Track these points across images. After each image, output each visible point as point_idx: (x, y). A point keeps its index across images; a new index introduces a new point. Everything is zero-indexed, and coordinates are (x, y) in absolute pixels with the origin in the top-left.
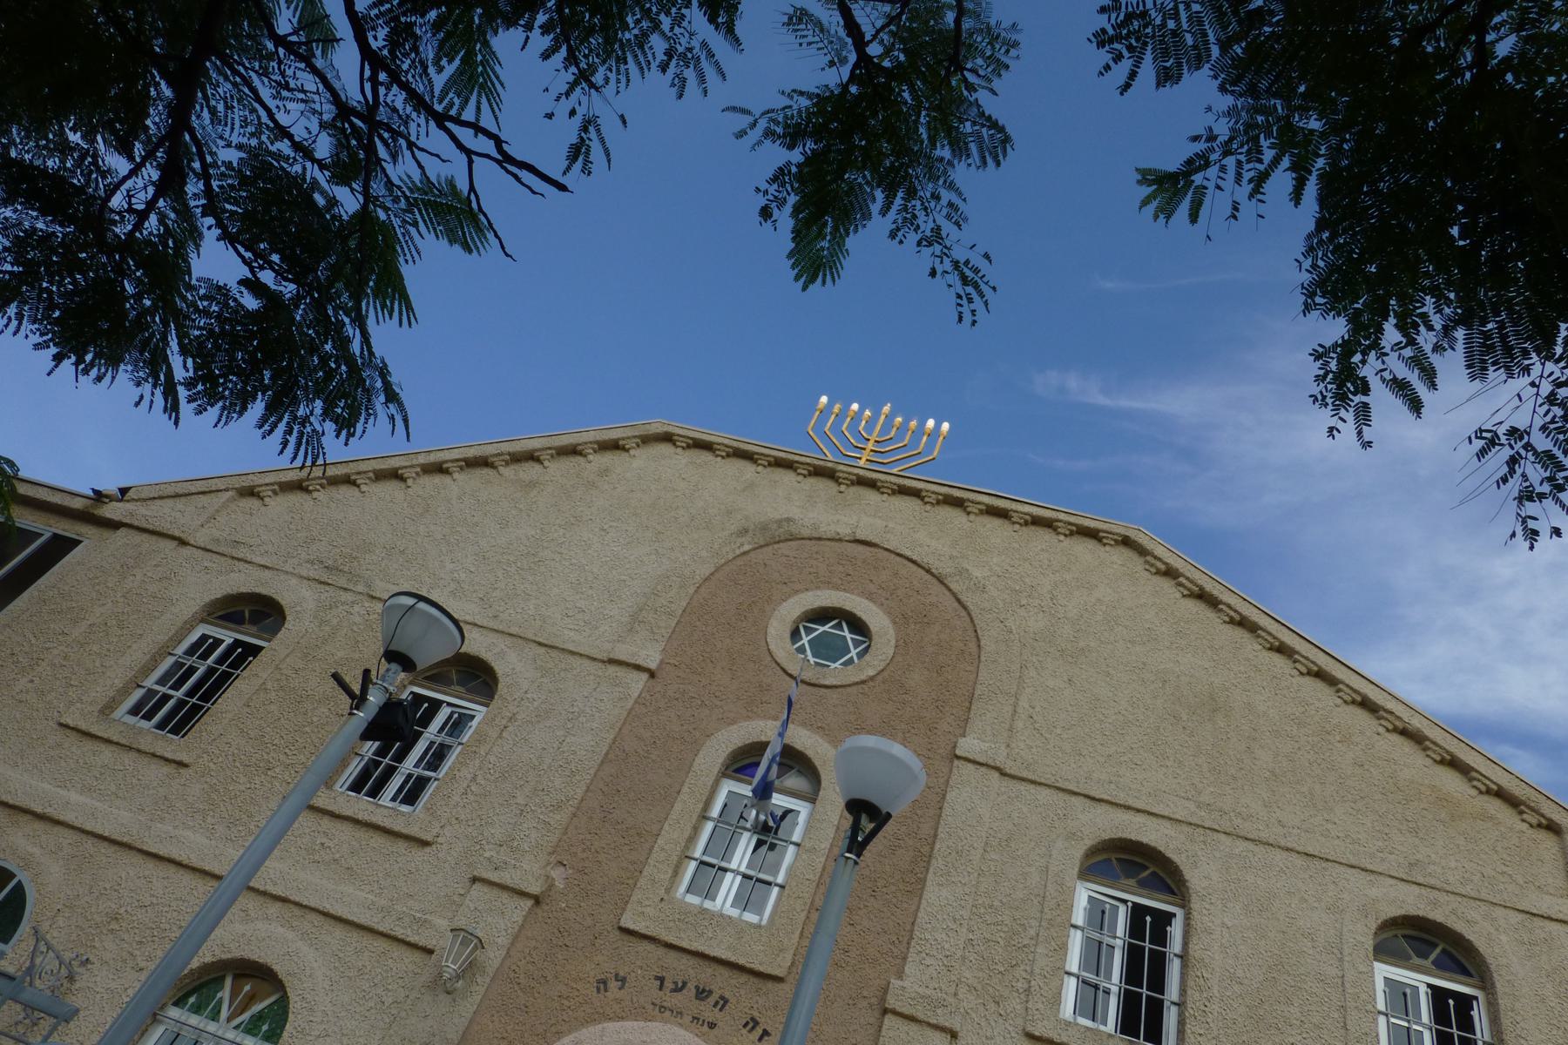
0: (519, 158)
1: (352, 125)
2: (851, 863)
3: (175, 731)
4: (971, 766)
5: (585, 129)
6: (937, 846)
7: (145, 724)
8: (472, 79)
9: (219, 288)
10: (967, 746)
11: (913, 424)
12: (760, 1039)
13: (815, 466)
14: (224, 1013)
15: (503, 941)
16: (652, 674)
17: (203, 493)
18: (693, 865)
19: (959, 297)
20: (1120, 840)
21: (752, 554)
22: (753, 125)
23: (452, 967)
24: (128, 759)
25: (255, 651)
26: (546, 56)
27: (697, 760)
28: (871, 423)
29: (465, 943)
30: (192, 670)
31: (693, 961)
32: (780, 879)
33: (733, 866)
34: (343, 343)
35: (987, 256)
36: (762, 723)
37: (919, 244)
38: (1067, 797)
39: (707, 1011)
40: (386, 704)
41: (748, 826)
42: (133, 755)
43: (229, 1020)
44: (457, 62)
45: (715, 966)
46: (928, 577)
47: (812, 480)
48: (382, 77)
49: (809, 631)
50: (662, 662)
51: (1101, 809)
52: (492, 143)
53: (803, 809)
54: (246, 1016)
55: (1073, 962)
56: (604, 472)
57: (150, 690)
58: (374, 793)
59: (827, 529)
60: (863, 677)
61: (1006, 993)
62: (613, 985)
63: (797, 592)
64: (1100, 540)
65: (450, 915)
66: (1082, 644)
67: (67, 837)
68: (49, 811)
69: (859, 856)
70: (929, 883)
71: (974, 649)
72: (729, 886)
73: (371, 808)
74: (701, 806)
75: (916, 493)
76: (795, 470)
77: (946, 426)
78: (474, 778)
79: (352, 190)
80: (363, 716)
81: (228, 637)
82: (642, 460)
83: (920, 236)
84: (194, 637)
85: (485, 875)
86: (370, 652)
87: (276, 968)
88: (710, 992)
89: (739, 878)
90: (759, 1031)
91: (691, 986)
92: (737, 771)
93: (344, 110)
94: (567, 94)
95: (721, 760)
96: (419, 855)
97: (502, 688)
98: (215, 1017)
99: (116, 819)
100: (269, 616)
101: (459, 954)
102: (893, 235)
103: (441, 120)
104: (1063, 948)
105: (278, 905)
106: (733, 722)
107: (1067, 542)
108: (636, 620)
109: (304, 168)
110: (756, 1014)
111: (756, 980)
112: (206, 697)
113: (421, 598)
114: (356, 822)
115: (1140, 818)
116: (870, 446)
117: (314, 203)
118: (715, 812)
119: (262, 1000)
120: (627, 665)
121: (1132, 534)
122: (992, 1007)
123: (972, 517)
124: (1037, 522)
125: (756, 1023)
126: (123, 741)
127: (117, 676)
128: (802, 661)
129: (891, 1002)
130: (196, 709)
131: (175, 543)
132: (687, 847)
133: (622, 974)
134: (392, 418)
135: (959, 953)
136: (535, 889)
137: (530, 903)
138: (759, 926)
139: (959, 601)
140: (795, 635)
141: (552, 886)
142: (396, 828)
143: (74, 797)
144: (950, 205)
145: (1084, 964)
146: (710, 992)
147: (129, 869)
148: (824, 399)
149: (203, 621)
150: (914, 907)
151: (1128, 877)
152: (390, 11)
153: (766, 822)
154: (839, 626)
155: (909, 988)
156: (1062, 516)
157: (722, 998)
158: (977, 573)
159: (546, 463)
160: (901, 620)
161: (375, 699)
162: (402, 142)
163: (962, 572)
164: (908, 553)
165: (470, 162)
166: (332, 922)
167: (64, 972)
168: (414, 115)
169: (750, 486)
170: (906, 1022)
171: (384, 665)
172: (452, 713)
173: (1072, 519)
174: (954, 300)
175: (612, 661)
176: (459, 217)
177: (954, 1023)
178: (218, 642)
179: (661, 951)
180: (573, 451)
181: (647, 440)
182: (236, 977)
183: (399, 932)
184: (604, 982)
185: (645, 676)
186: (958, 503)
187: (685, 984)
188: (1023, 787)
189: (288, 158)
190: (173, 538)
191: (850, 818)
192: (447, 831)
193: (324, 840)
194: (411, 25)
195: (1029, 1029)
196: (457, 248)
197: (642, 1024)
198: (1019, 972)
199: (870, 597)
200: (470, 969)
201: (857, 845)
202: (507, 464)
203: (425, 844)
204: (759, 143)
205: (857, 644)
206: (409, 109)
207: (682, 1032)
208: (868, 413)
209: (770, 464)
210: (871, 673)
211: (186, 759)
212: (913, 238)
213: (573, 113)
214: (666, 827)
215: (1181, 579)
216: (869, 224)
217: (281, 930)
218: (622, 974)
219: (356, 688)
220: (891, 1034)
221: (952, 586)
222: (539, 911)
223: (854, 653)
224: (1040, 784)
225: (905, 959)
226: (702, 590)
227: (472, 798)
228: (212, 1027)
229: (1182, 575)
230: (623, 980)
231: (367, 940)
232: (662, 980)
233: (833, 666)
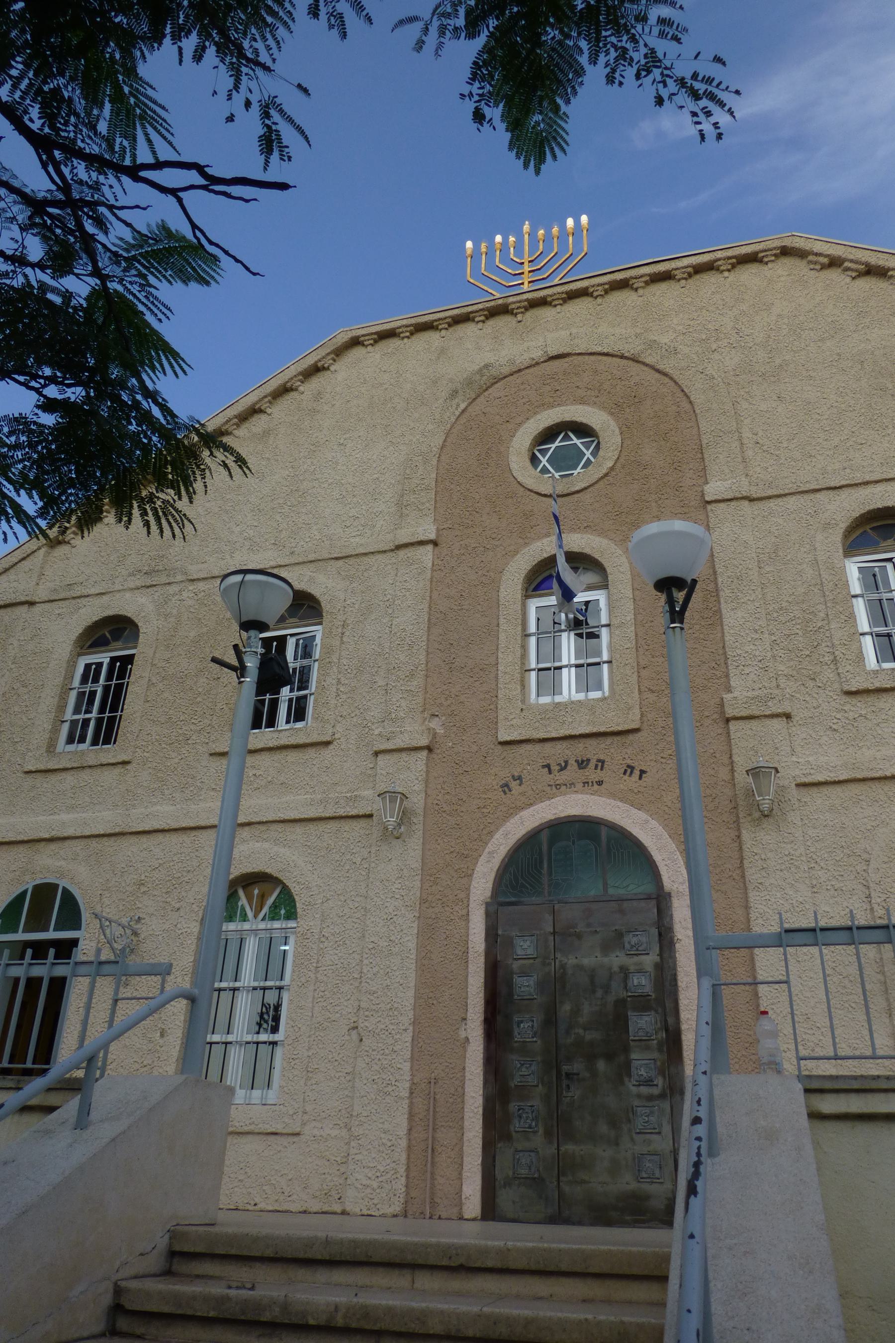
0: (228, 176)
1: (50, 216)
2: (678, 630)
3: (107, 741)
4: (722, 505)
5: (266, 115)
6: (720, 580)
7: (82, 747)
8: (129, 112)
9: (16, 419)
10: (713, 489)
11: (555, 230)
12: (640, 778)
13: (487, 309)
14: (250, 914)
15: (419, 787)
16: (435, 543)
17: (24, 559)
18: (533, 674)
19: (694, 114)
20: (869, 512)
21: (470, 409)
22: (426, 30)
23: (392, 821)
24: (85, 775)
25: (130, 659)
26: (198, 57)
27: (502, 595)
28: (518, 246)
29: (393, 800)
30: (93, 694)
31: (565, 744)
32: (605, 657)
33: (565, 662)
34: (146, 418)
35: (718, 60)
36: (539, 544)
37: (638, 76)
38: (812, 496)
39: (592, 774)
40: (261, 664)
41: (563, 627)
42: (88, 771)
43: (255, 917)
44: (108, 106)
45: (583, 740)
46: (624, 362)
47: (491, 322)
48: (57, 153)
49: (543, 452)
50: (438, 530)
51: (844, 493)
52: (194, 173)
53: (600, 596)
54: (266, 909)
55: (864, 624)
56: (318, 396)
57: (71, 721)
58: (271, 723)
59: (524, 359)
60: (604, 471)
61: (818, 669)
62: (514, 784)
63: (520, 425)
64: (761, 261)
65: (371, 785)
66: (778, 361)
67: (77, 846)
68: (54, 833)
69: (682, 622)
70: (724, 611)
71: (687, 406)
72: (568, 678)
73: (275, 735)
74: (520, 628)
75: (583, 293)
76: (473, 320)
77: (584, 219)
78: (339, 682)
79: (77, 275)
80: (250, 680)
81: (104, 658)
82: (343, 371)
83: (635, 67)
84: (80, 669)
85: (383, 747)
86: (234, 634)
87: (268, 871)
88: (588, 760)
89: (573, 670)
90: (637, 773)
91: (572, 761)
92: (535, 589)
93: (37, 205)
94: (236, 87)
95: (520, 587)
96: (327, 753)
97: (325, 606)
98: (244, 918)
99: (103, 819)
100: (125, 629)
101: (392, 810)
102: (610, 79)
103: (134, 172)
104: (852, 617)
105: (247, 828)
106: (516, 552)
107: (732, 277)
108: (401, 507)
109: (26, 276)
110: (629, 762)
111: (619, 738)
112: (114, 709)
113: (245, 572)
115: (880, 488)
116: (527, 268)
117: (50, 303)
118: (532, 628)
119: (271, 895)
120: (412, 544)
121: (787, 242)
122: (811, 684)
123: (640, 291)
124: (699, 269)
125: (632, 768)
126: (75, 765)
127: (44, 723)
128: (548, 480)
129: (730, 712)
130: (112, 720)
131: (26, 607)
132: (523, 664)
133: (516, 774)
134: (225, 465)
135: (769, 654)
136: (424, 742)
137: (425, 753)
138: (604, 699)
139: (658, 371)
140: (534, 460)
141: (435, 735)
142: (301, 742)
143: (65, 817)
144: (662, 21)
145: (873, 622)
146: (588, 760)
147: (131, 848)
148: (469, 244)
149: (79, 655)
150: (719, 635)
151: (885, 539)
152: (30, 85)
153: (575, 618)
154: (567, 438)
155: (741, 693)
156: (719, 255)
157: (599, 761)
158: (664, 339)
159: (269, 411)
160: (615, 410)
161: (252, 663)
162: (102, 209)
163: (652, 345)
164: (599, 349)
165: (180, 201)
166: (291, 824)
167: (128, 932)
168: (102, 178)
169: (443, 351)
170: (747, 722)
171: (244, 634)
172: (298, 640)
173: (730, 253)
174: (689, 118)
175: (399, 547)
176: (184, 256)
177: (786, 707)
178: (100, 665)
179: (538, 747)
180: (284, 390)
181: (339, 352)
182: (244, 888)
183: (341, 812)
184: (507, 785)
185: (430, 547)
186: (623, 285)
187: (566, 762)
188: (772, 503)
189: (7, 273)
191: (663, 597)
192: (339, 728)
193: (254, 772)
194: (56, 91)
195: (846, 688)
196: (193, 285)
197: (548, 802)
198: (823, 649)
199: (582, 401)
200: (405, 817)
201: (677, 615)
202: (238, 425)
203: (327, 743)
204: (440, 46)
205: (587, 445)
206: (94, 175)
207: (580, 796)
208: (512, 239)
209: (450, 325)
210: (610, 464)
211: (126, 758)
212: (630, 72)
213: (248, 104)
214: (500, 655)
215: (846, 264)
216: (585, 79)
217: (258, 845)
218: (516, 774)
219: (234, 662)
220: (739, 734)
221: (647, 361)
222: (434, 756)
223: (588, 454)
224: (785, 495)
225: (727, 676)
226: (443, 458)
227: (345, 696)
228: (246, 926)
229: (845, 260)
230: (520, 778)
231: (322, 826)
232: (548, 766)
233: (575, 472)
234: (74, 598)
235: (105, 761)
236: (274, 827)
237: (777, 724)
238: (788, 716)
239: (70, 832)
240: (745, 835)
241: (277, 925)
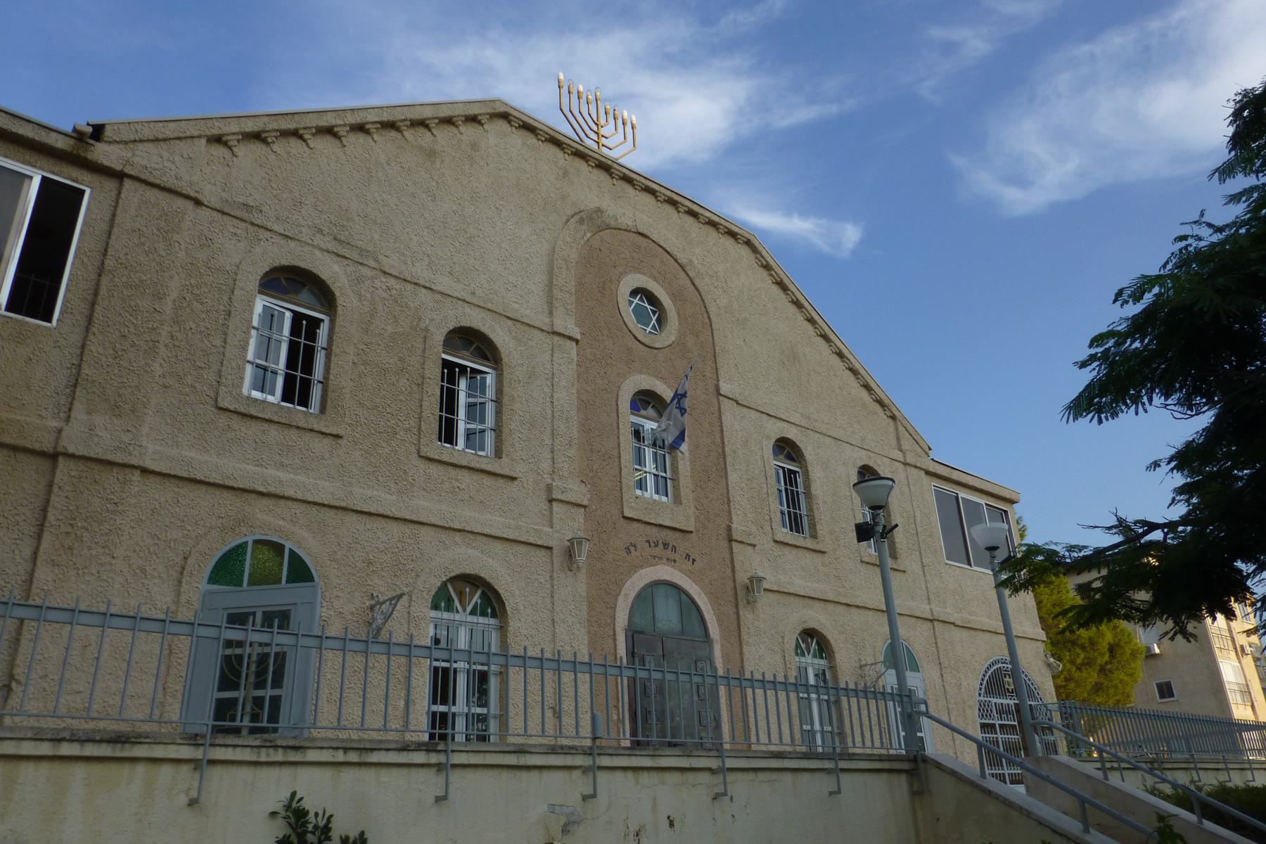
13: (600, 161)
47: (596, 171)
62: (632, 549)
68: (272, 489)
99: (325, 490)
114: (470, 468)
120: (564, 336)
131: (189, 205)
143: (271, 472)
179: (643, 526)
183: (532, 540)
190: (188, 197)
211: (340, 432)
228: (457, 617)
234: (253, 224)
235: (316, 427)
237: (750, 548)
238: (754, 546)
239: (290, 492)
240: (741, 613)
241: (481, 620)
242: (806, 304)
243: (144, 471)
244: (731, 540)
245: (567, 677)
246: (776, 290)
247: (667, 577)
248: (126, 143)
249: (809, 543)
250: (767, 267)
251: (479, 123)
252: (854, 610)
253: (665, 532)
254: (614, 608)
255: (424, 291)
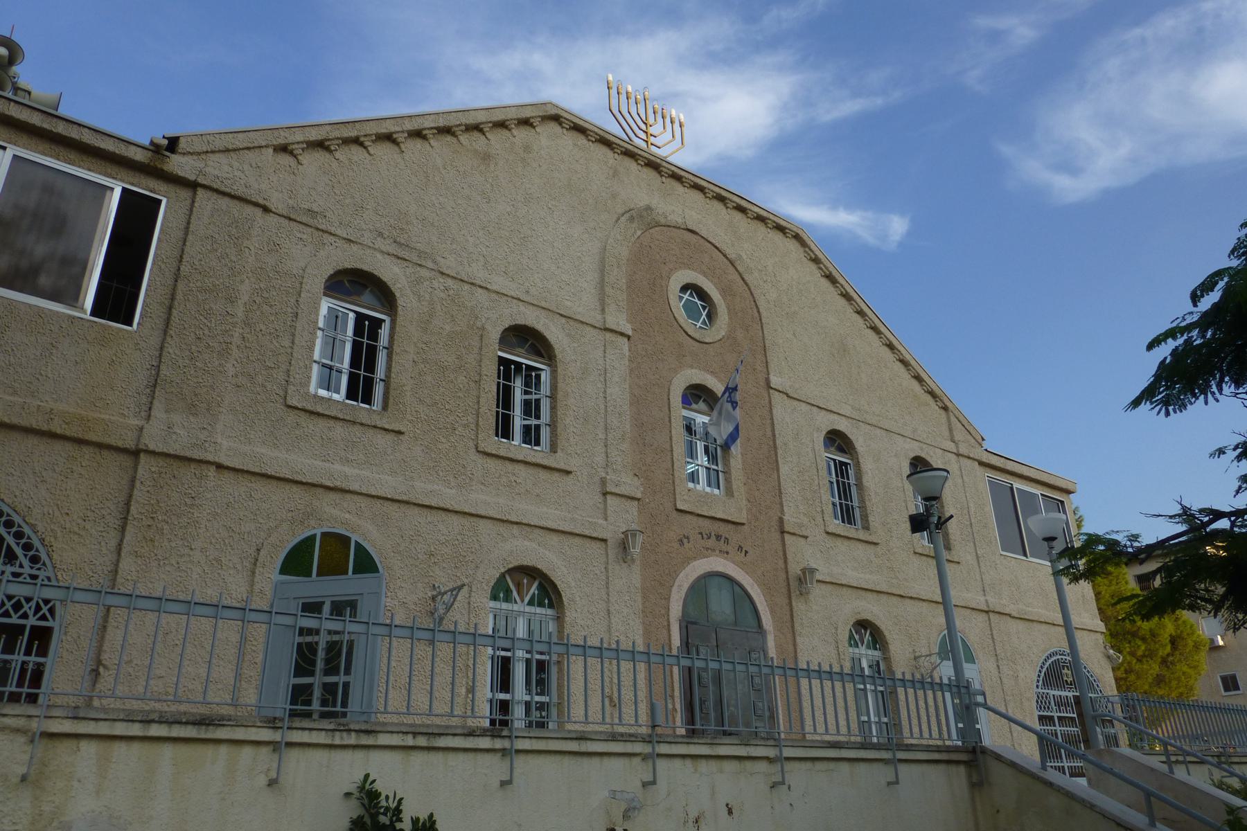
68: (338, 484)
73: (533, 453)
99: (388, 484)
114: (526, 463)
120: (616, 332)
131: (258, 212)
143: (337, 467)
179: (695, 518)
183: (587, 533)
190: (256, 205)
211: (403, 429)
228: (516, 607)
234: (318, 229)
235: (379, 424)
236: (537, 531)
238: (806, 537)
239: (355, 486)
241: (539, 610)
242: (855, 296)
243: (220, 466)
244: (783, 532)
245: (804, 682)
246: (825, 283)
247: (721, 569)
248: (199, 154)
249: (862, 535)
250: (816, 260)
251: (531, 125)
252: (908, 601)
253: (717, 524)
254: (668, 599)
255: (480, 290)
